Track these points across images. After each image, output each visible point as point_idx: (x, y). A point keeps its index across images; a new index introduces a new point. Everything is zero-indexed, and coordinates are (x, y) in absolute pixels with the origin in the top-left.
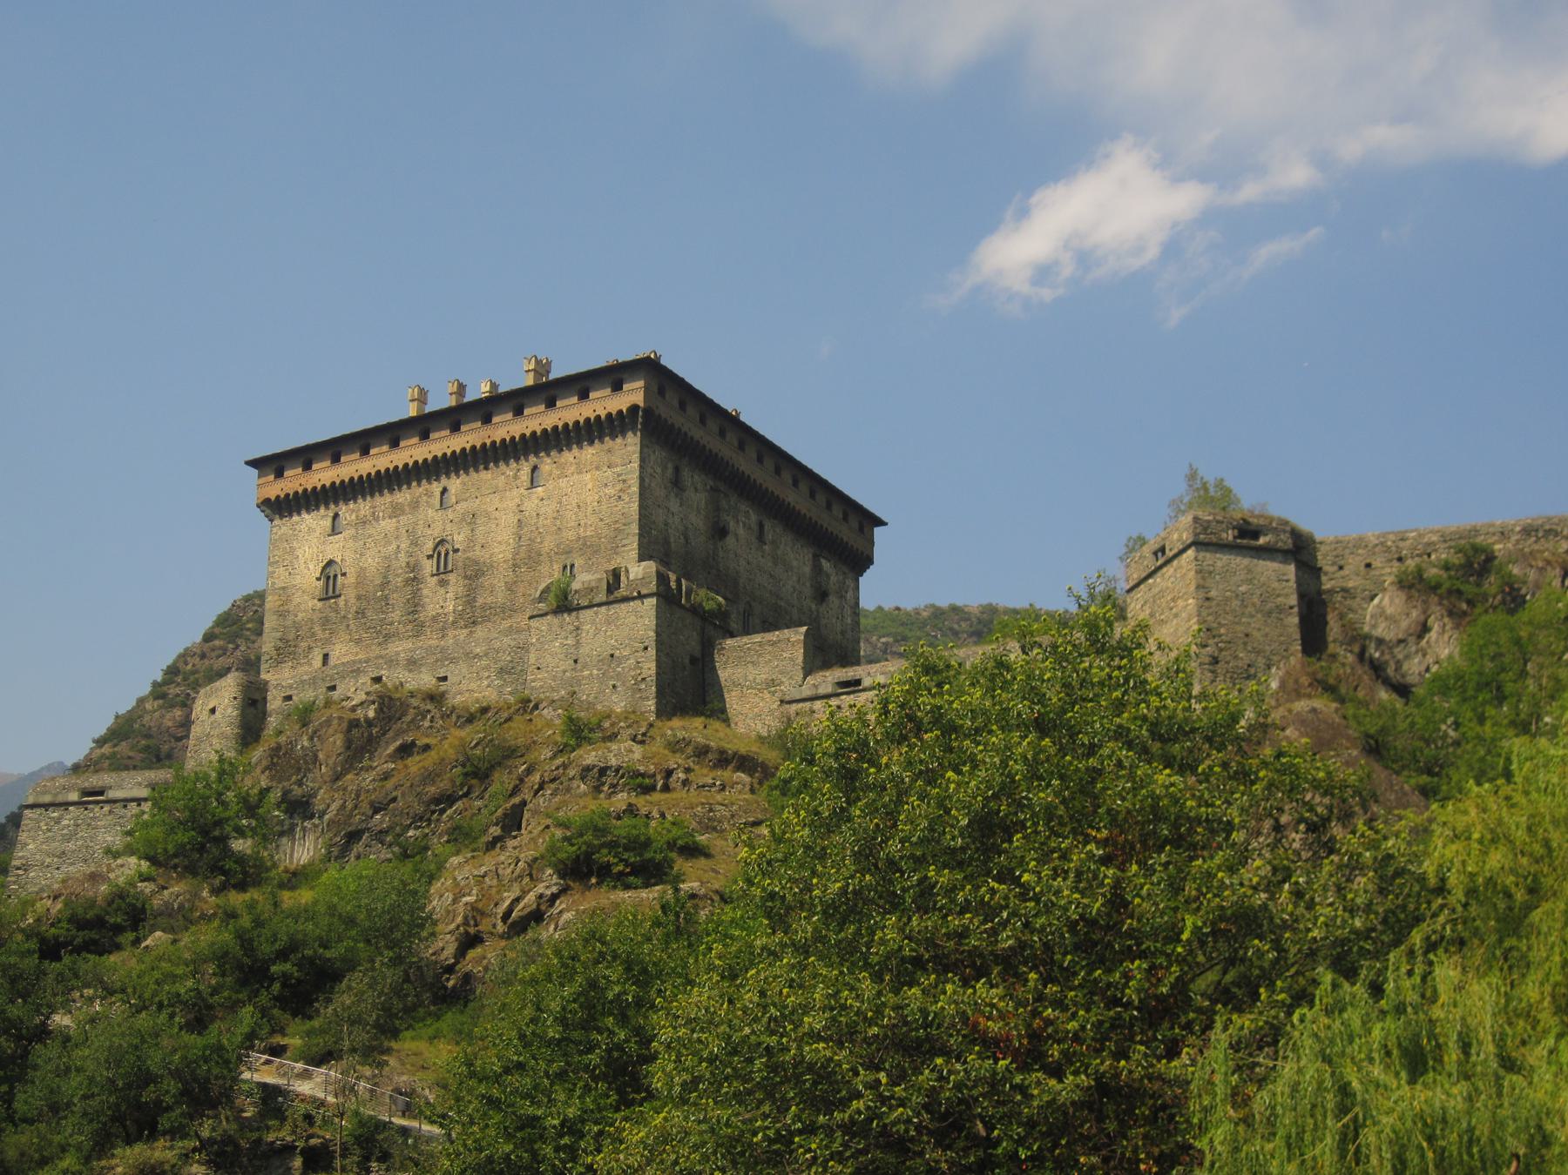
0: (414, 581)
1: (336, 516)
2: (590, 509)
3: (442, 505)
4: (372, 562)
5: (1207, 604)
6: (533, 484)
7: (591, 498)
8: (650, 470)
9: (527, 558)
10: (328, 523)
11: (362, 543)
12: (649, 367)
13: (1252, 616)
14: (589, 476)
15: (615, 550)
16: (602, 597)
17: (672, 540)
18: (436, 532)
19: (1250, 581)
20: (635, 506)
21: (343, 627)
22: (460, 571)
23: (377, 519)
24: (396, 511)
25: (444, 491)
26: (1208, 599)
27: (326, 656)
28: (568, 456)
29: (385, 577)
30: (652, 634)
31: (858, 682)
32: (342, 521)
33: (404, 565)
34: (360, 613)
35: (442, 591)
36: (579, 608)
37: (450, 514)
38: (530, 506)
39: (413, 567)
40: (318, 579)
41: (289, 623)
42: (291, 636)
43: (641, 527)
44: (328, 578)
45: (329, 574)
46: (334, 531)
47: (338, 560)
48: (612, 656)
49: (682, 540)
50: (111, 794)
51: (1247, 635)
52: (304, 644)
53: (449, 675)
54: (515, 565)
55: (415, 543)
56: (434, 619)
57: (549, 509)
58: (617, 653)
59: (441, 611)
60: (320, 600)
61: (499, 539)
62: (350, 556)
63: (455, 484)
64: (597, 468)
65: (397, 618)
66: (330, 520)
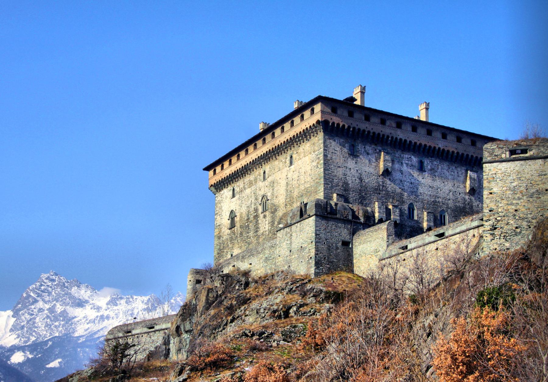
0: (256, 217)
1: (234, 190)
2: (308, 174)
3: (264, 179)
4: (244, 210)
5: (491, 195)
6: (291, 163)
7: (308, 168)
8: (331, 150)
9: (290, 200)
10: (231, 193)
11: (241, 201)
12: (319, 99)
13: (519, 199)
14: (307, 158)
15: (316, 192)
16: (298, 218)
17: (350, 182)
18: (262, 193)
19: (519, 179)
20: (322, 170)
21: (236, 241)
22: (270, 210)
23: (245, 189)
24: (251, 184)
25: (264, 173)
26: (491, 193)
27: (232, 255)
28: (301, 149)
29: (248, 216)
30: (314, 235)
31: (406, 247)
32: (237, 189)
33: (253, 209)
34: (241, 234)
35: (264, 220)
36: (291, 225)
37: (267, 183)
38: (290, 176)
39: (256, 210)
40: (229, 220)
41: (221, 241)
42: (222, 248)
43: (325, 179)
44: (232, 218)
45: (232, 216)
46: (234, 196)
47: (234, 210)
48: (301, 247)
49: (358, 181)
50: (134, 332)
51: (516, 210)
52: (225, 251)
53: (252, 263)
54: (286, 205)
55: (256, 199)
56: (262, 234)
57: (295, 176)
58: (303, 245)
59: (264, 230)
60: (230, 229)
61: (281, 193)
62: (238, 207)
63: (267, 167)
64: (310, 153)
65: (251, 235)
66: (232, 191)
